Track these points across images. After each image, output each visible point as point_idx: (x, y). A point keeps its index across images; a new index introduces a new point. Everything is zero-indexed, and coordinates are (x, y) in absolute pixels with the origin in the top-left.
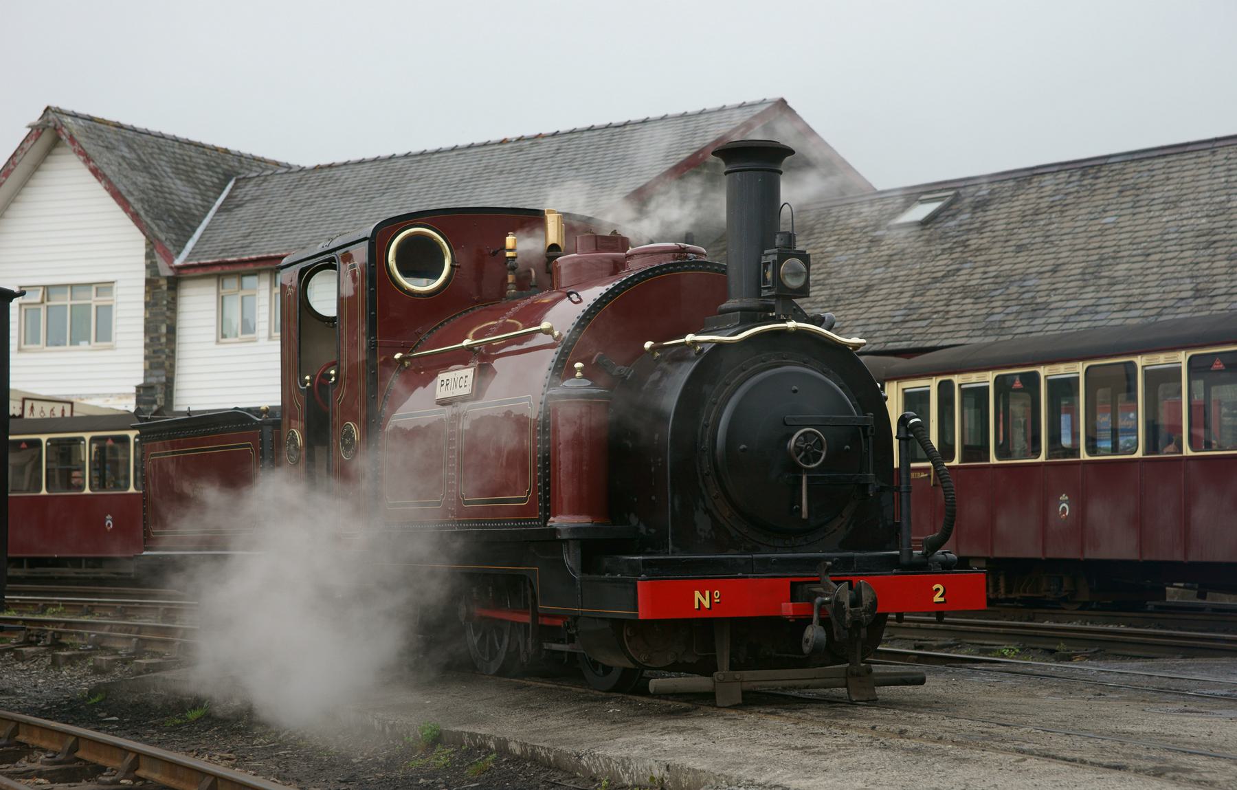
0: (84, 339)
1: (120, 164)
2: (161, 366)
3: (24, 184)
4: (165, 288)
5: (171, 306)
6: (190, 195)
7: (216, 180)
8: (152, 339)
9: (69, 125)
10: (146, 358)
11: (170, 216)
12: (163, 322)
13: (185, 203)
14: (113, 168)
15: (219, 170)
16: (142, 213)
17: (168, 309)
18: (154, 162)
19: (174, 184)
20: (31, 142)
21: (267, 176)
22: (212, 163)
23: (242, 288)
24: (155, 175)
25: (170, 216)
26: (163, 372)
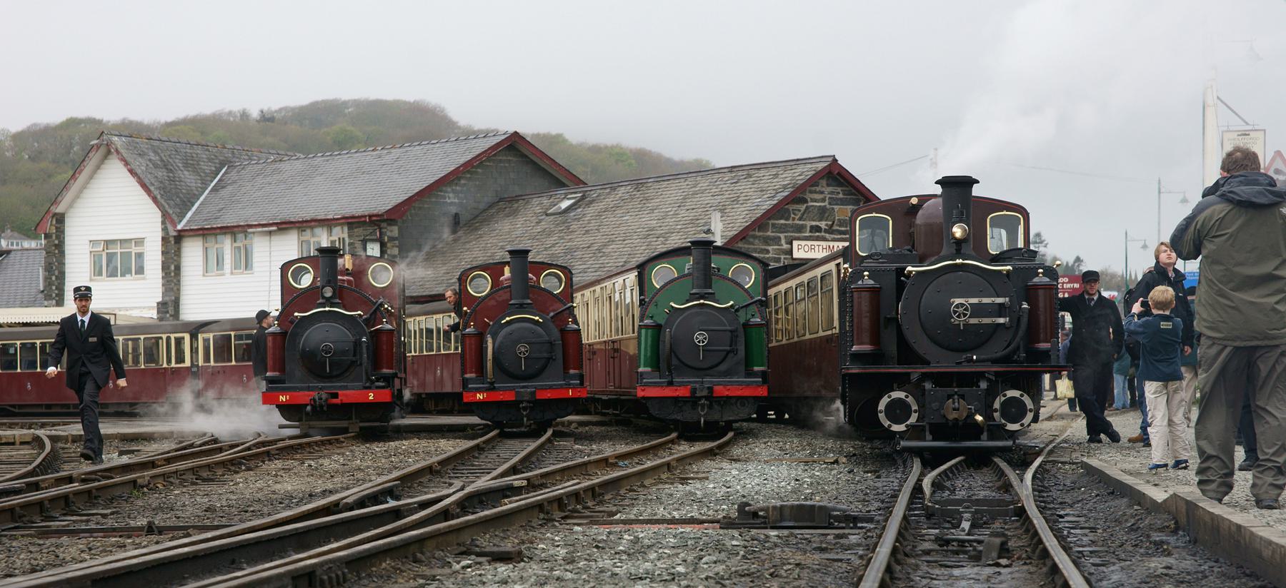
0: (128, 274)
1: (147, 165)
2: (172, 289)
3: (91, 177)
4: (173, 242)
5: (177, 253)
6: (193, 181)
7: (214, 169)
8: (166, 274)
9: (116, 143)
10: (163, 285)
11: (177, 197)
12: (172, 263)
13: (189, 187)
14: (142, 168)
16: (159, 197)
17: (175, 255)
18: (171, 160)
19: (184, 174)
20: (94, 153)
21: (245, 165)
22: (212, 157)
23: (217, 243)
24: (171, 170)
25: (180, 198)
26: (172, 293)
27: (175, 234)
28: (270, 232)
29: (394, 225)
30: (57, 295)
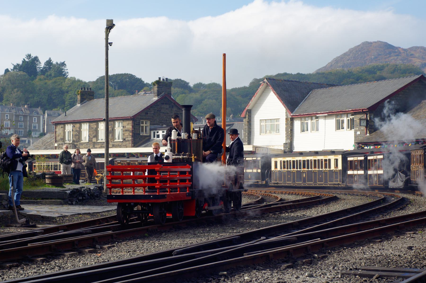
4: (290, 120)
8: (287, 132)
15: (308, 89)
27: (290, 117)
28: (325, 116)
29: (372, 113)
30: (248, 140)
